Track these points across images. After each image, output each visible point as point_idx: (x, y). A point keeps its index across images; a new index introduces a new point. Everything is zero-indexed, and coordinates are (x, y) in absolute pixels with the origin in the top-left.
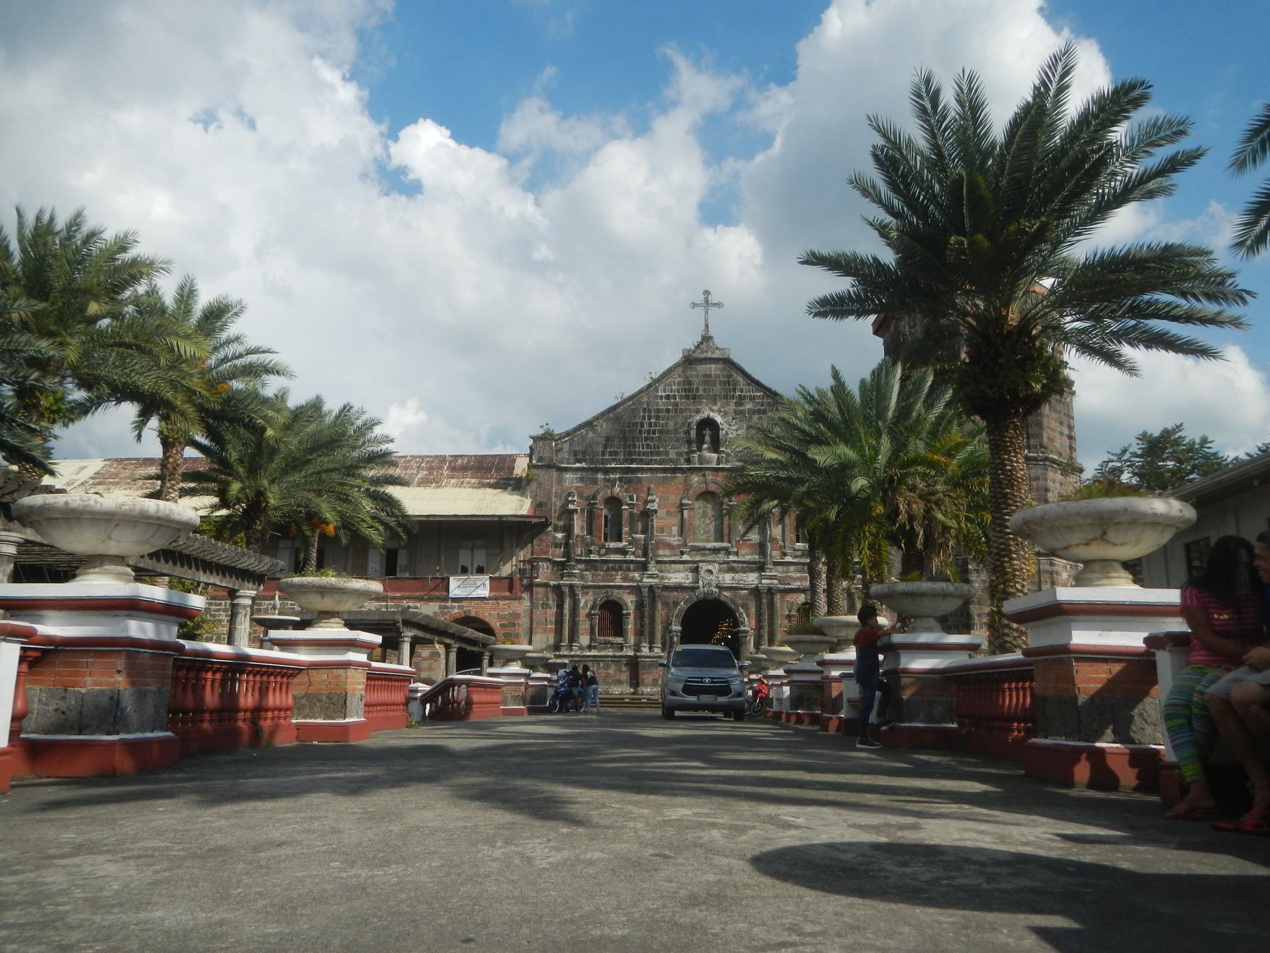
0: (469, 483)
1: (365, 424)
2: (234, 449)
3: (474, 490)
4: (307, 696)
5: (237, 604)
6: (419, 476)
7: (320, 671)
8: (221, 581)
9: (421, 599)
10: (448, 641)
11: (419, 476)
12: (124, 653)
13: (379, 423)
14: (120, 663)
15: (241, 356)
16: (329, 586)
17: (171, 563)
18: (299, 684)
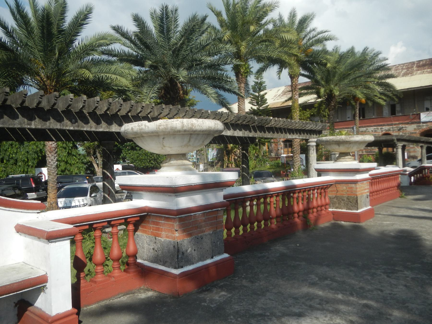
0: (427, 71)
1: (374, 54)
2: (319, 75)
3: (430, 74)
4: (336, 197)
5: (309, 145)
6: (403, 72)
7: (342, 185)
8: (299, 136)
9: (408, 124)
10: (421, 144)
11: (403, 72)
12: (178, 219)
13: (381, 53)
14: (176, 225)
15: (316, 36)
16: (341, 140)
17: (271, 133)
18: (332, 191)
